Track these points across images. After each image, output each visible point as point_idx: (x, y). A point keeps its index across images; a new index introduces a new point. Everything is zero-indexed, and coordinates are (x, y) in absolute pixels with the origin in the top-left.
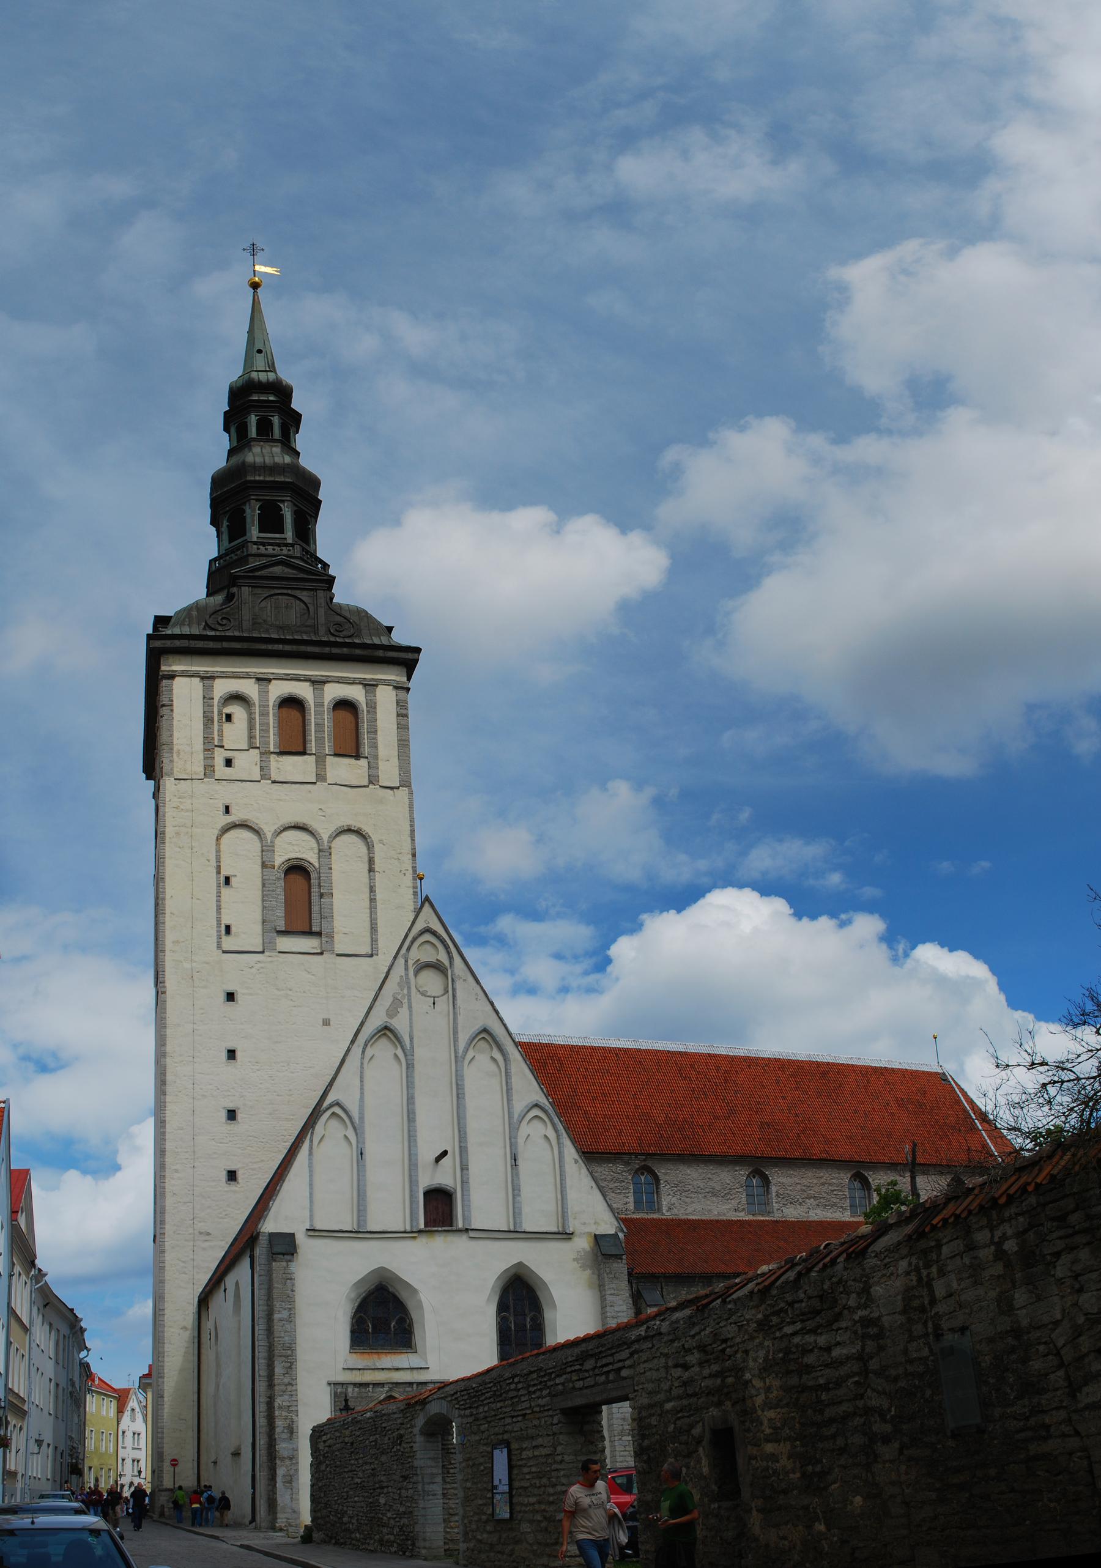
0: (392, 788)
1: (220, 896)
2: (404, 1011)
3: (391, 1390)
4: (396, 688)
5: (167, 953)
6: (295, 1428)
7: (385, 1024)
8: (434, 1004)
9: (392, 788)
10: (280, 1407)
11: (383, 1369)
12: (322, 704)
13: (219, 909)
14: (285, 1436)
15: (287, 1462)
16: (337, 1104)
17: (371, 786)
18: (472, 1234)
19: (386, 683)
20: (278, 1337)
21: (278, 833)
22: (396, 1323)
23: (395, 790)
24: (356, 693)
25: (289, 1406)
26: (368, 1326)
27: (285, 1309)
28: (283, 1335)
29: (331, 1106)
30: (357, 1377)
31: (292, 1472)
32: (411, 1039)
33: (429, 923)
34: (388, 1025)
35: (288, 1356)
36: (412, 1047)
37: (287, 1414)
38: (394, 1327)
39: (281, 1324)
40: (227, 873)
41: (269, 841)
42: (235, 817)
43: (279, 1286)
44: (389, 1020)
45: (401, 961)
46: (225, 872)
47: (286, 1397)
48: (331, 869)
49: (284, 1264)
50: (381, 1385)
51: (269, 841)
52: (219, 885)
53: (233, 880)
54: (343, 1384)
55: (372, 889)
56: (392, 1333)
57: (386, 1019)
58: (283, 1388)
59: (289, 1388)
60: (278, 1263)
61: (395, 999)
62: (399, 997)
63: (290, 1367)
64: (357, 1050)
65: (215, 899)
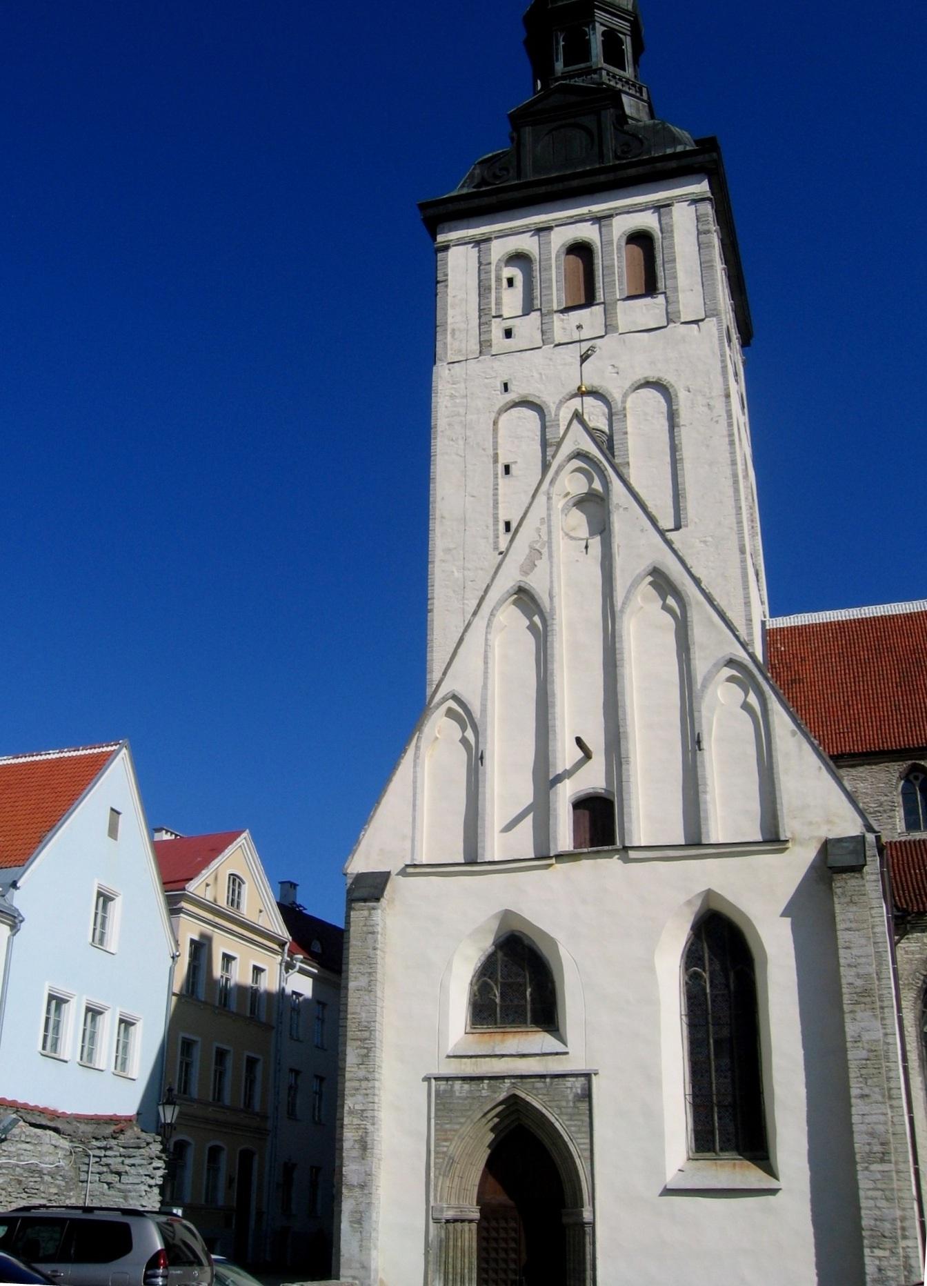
0: (696, 322)
1: (497, 489)
2: (542, 564)
3: (514, 1085)
4: (695, 202)
5: (437, 564)
6: (369, 1142)
7: (518, 585)
8: (587, 547)
9: (696, 322)
10: (351, 1112)
11: (503, 1056)
12: (611, 242)
13: (496, 503)
14: (355, 1153)
15: (357, 1192)
16: (455, 697)
17: (672, 325)
18: (632, 854)
19: (680, 199)
20: (353, 1014)
21: (561, 403)
23: (700, 323)
24: (648, 221)
25: (362, 1111)
26: (495, 995)
27: (363, 974)
28: (358, 1011)
29: (444, 700)
30: (469, 1068)
31: (362, 1208)
32: (551, 597)
33: (579, 444)
34: (522, 584)
35: (366, 1039)
36: (552, 609)
37: (359, 1122)
39: (357, 994)
40: (506, 462)
41: (553, 415)
42: (512, 396)
43: (357, 943)
44: (523, 579)
45: (541, 499)
46: (502, 461)
47: (360, 1098)
48: (626, 433)
49: (366, 913)
51: (553, 415)
53: (513, 469)
54: (447, 1079)
55: (674, 448)
57: (519, 578)
58: (356, 1084)
59: (364, 1084)
60: (357, 912)
61: (532, 549)
62: (537, 547)
63: (367, 1056)
64: (480, 623)
65: (491, 492)
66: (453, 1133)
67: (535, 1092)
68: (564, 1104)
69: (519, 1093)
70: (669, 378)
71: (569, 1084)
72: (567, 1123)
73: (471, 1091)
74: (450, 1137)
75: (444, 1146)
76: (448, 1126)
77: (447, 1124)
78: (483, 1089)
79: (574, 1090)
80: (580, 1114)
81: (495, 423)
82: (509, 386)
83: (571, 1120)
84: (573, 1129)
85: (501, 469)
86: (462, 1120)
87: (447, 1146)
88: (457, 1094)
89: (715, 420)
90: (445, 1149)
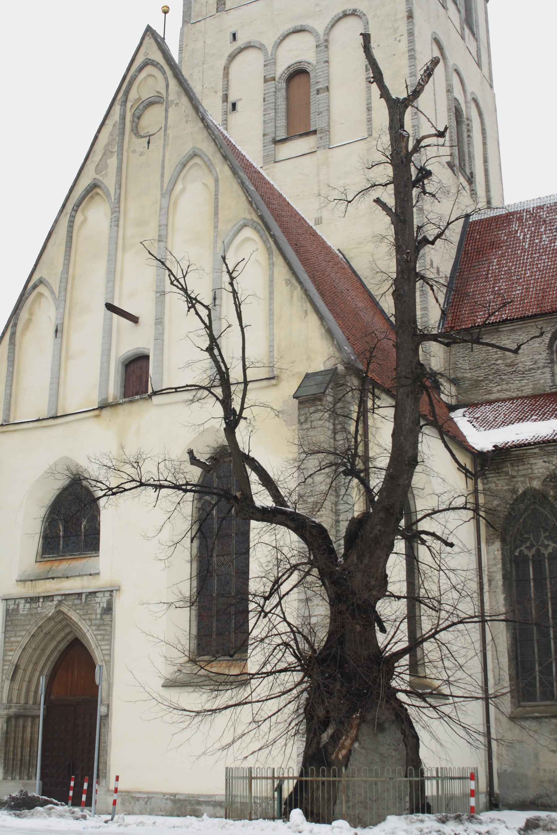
22: (87, 522)
26: (60, 530)
38: (85, 527)
41: (269, 55)
44: (98, 177)
46: (231, 99)
50: (49, 598)
51: (269, 55)
52: (226, 113)
53: (238, 106)
56: (83, 535)
66: (17, 644)
67: (74, 608)
68: (93, 617)
69: (64, 609)
70: (361, 7)
71: (98, 600)
72: (95, 632)
73: (30, 609)
74: (15, 647)
75: (10, 655)
76: (13, 639)
77: (13, 637)
78: (39, 607)
79: (101, 605)
80: (104, 625)
81: (226, 69)
82: (237, 36)
83: (98, 630)
84: (99, 637)
85: (230, 106)
86: (23, 633)
87: (12, 656)
88: (21, 612)
89: (398, 39)
90: (10, 658)
